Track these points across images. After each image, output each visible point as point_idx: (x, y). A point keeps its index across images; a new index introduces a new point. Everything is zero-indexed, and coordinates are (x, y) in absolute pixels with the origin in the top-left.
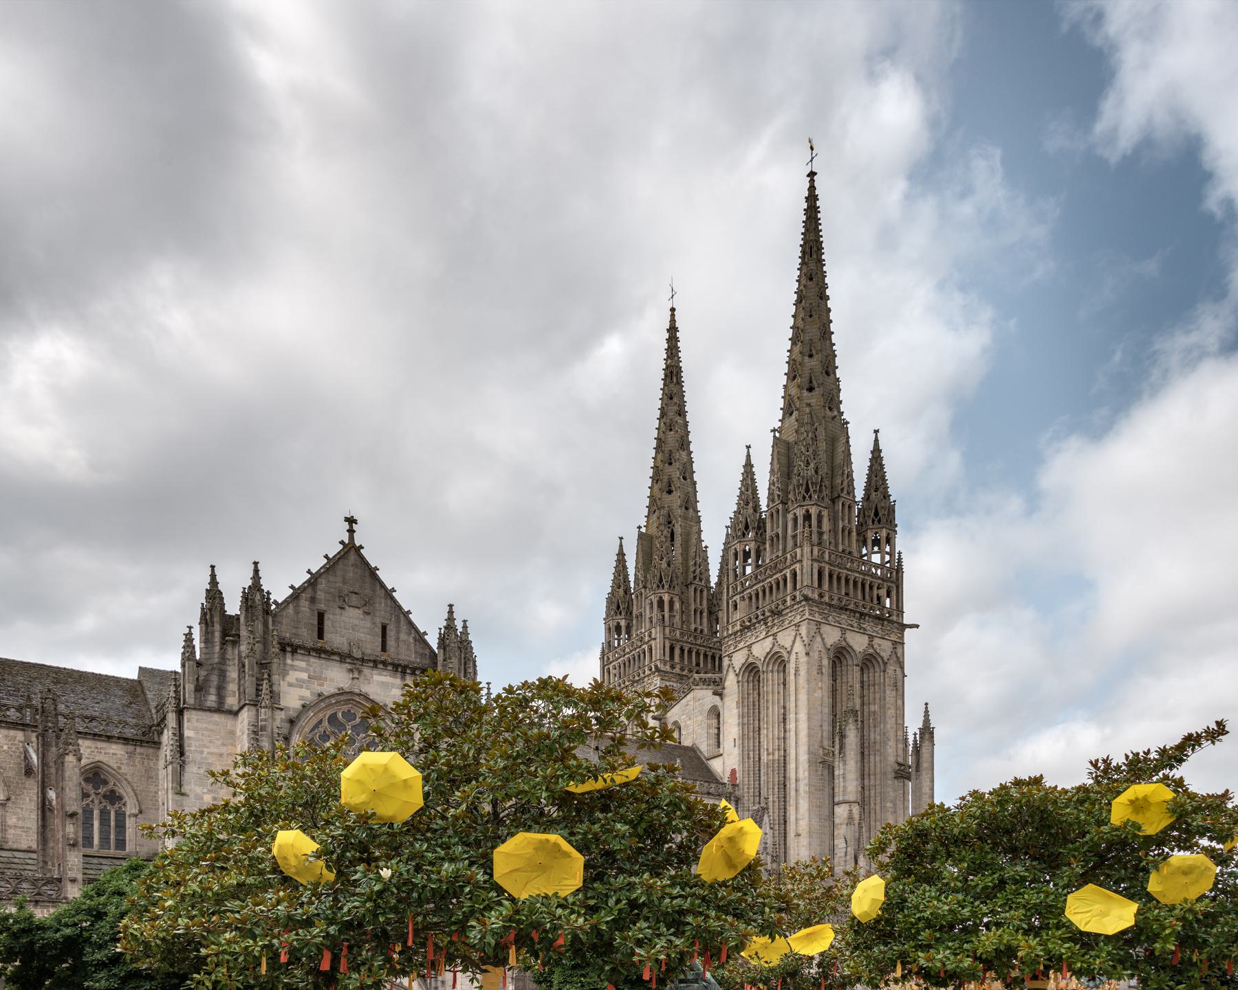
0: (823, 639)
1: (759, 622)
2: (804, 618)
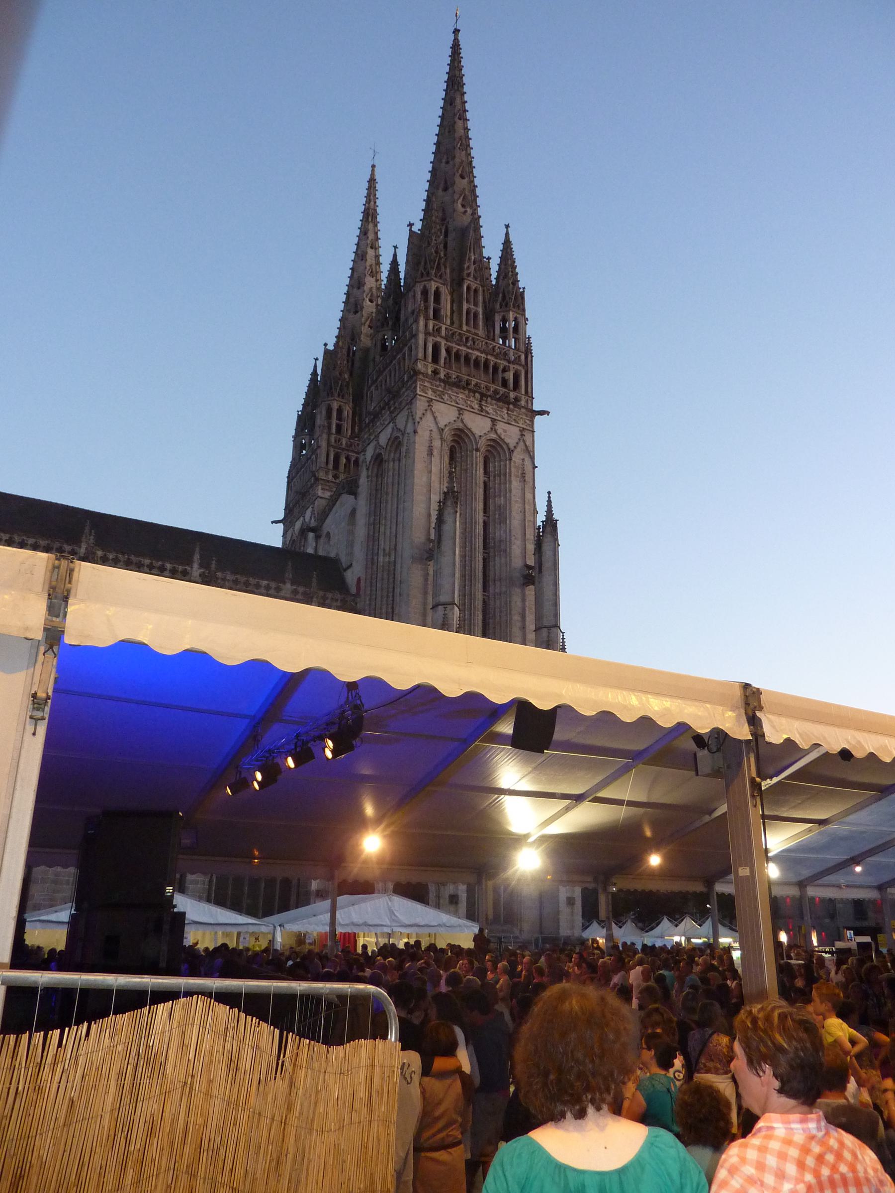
0: (435, 418)
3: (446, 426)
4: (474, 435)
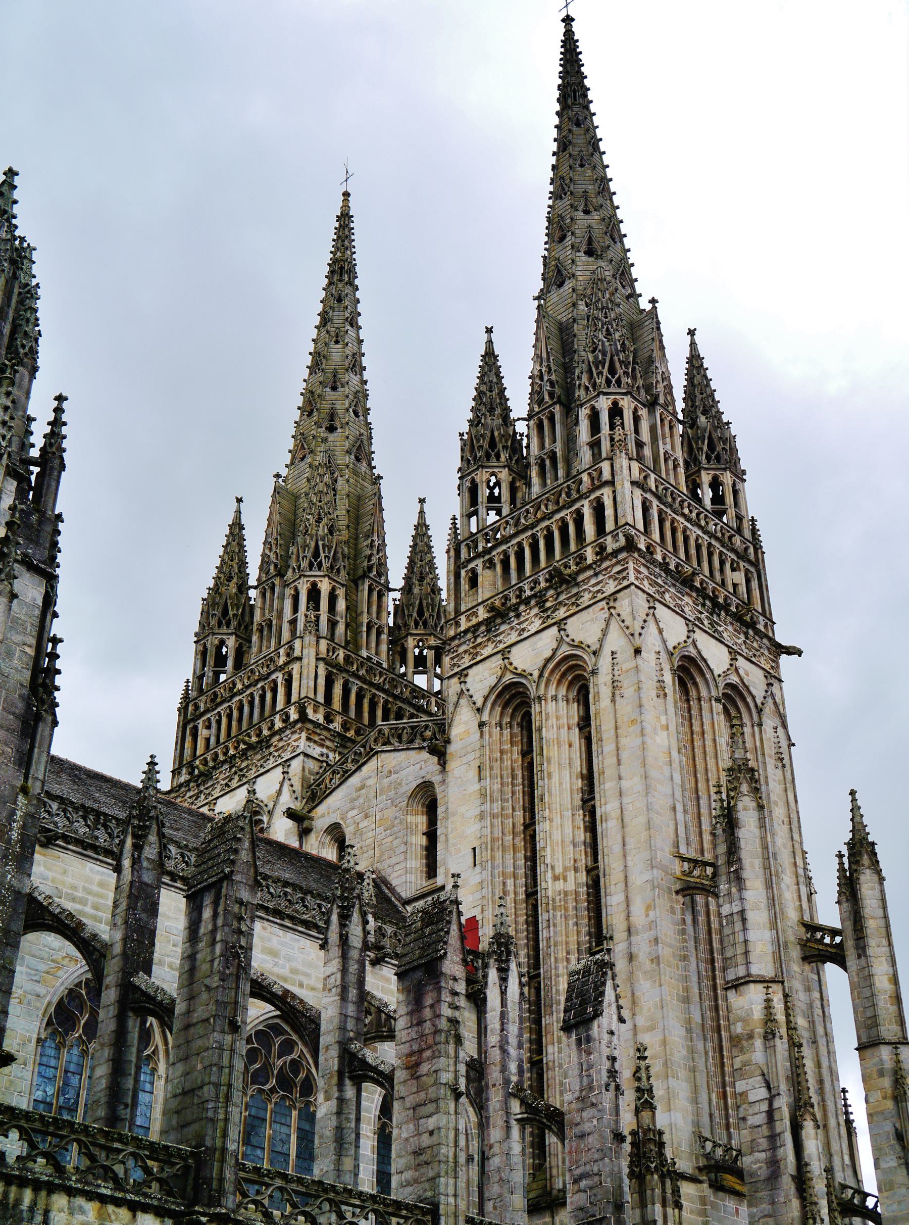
0: (661, 631)
1: (527, 602)
2: (625, 583)
3: (674, 648)
4: (711, 671)
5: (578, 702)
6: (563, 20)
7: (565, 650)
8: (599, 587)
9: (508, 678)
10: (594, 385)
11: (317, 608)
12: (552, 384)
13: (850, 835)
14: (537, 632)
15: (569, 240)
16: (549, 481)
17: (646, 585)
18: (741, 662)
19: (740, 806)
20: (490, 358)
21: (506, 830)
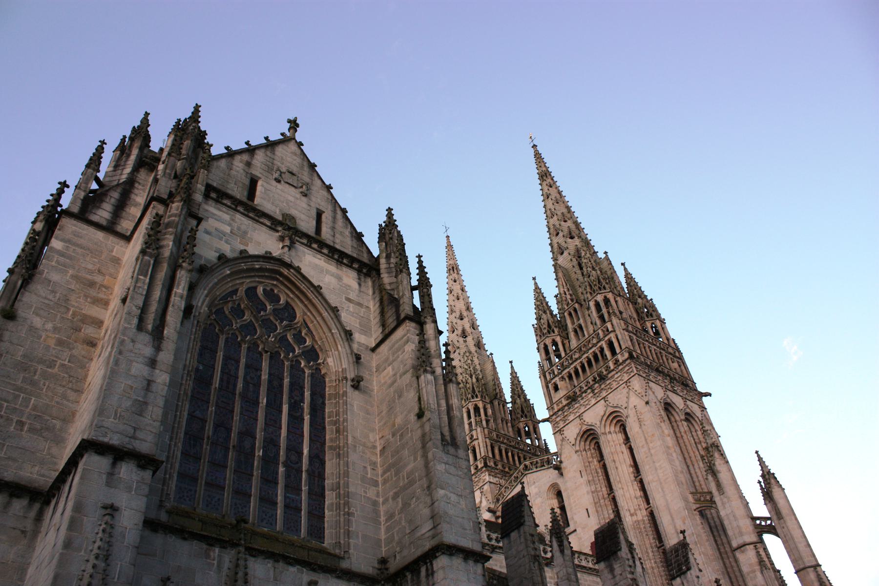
0: (654, 393)
2: (632, 374)
4: (678, 408)
5: (621, 432)
6: (533, 147)
7: (610, 410)
8: (620, 378)
9: (584, 428)
10: (594, 291)
11: (480, 415)
12: (571, 295)
13: (761, 472)
14: (594, 405)
15: (561, 234)
16: (580, 337)
17: (642, 374)
18: (688, 403)
19: (716, 463)
20: (538, 290)
21: (600, 498)
